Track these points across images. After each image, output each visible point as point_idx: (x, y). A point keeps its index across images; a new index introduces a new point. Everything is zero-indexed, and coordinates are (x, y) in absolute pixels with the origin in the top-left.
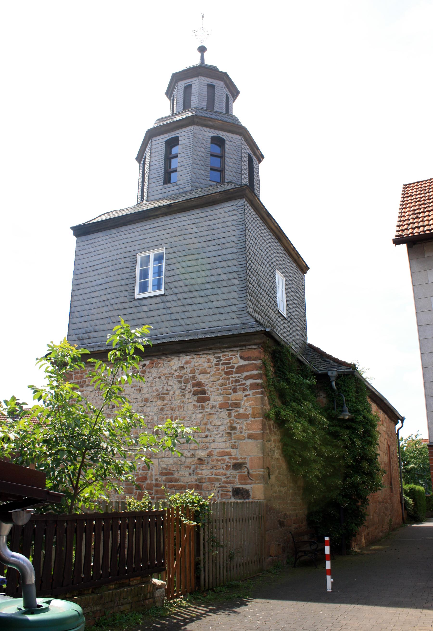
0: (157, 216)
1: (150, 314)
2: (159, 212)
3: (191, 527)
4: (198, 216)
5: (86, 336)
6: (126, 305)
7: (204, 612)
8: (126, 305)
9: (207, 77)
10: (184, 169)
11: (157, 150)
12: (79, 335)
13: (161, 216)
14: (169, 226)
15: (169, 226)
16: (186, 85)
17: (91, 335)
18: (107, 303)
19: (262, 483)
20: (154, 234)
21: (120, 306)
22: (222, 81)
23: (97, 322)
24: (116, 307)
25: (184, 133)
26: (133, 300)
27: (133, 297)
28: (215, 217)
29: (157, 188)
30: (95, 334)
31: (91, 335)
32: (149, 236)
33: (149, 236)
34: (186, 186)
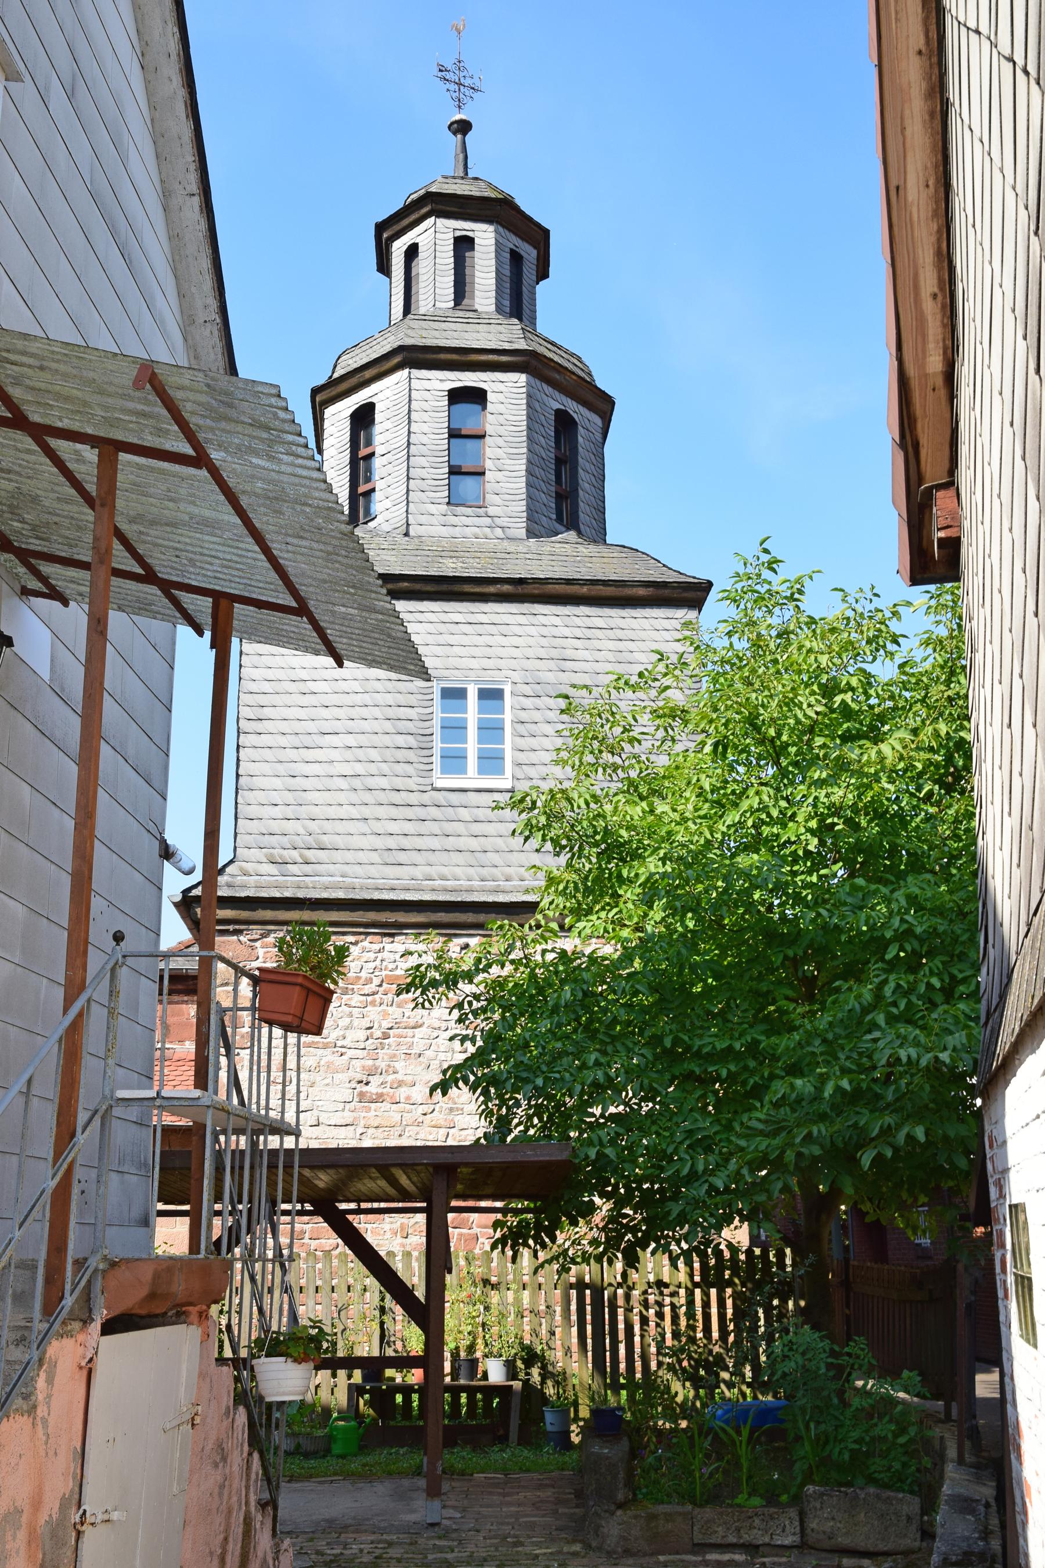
0: (484, 598)
1: (477, 828)
2: (492, 589)
3: (980, 1230)
4: (589, 622)
5: (295, 855)
6: (413, 798)
7: (256, 1456)
8: (413, 798)
9: (510, 230)
10: (504, 479)
11: (426, 406)
12: (272, 851)
13: (493, 598)
14: (518, 630)
15: (518, 630)
16: (458, 234)
17: (310, 855)
18: (357, 783)
19: (417, 1187)
20: (480, 640)
21: (397, 798)
22: (535, 248)
23: (328, 826)
24: (382, 797)
25: (500, 387)
26: (430, 788)
27: (427, 781)
28: (630, 634)
29: (433, 509)
30: (322, 855)
31: (310, 855)
32: (465, 640)
33: (465, 640)
34: (510, 525)
